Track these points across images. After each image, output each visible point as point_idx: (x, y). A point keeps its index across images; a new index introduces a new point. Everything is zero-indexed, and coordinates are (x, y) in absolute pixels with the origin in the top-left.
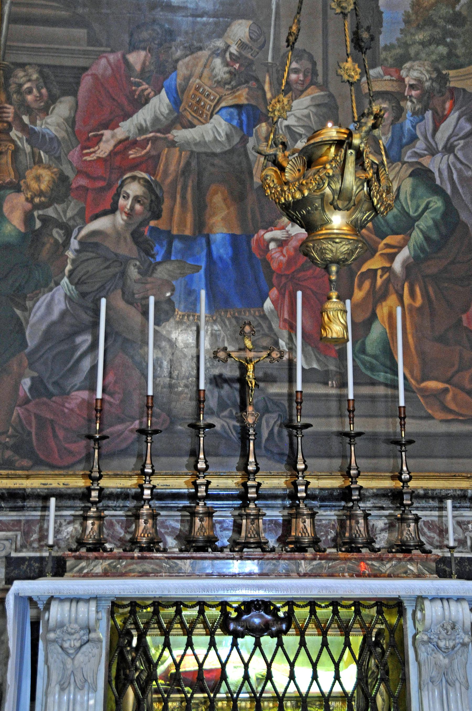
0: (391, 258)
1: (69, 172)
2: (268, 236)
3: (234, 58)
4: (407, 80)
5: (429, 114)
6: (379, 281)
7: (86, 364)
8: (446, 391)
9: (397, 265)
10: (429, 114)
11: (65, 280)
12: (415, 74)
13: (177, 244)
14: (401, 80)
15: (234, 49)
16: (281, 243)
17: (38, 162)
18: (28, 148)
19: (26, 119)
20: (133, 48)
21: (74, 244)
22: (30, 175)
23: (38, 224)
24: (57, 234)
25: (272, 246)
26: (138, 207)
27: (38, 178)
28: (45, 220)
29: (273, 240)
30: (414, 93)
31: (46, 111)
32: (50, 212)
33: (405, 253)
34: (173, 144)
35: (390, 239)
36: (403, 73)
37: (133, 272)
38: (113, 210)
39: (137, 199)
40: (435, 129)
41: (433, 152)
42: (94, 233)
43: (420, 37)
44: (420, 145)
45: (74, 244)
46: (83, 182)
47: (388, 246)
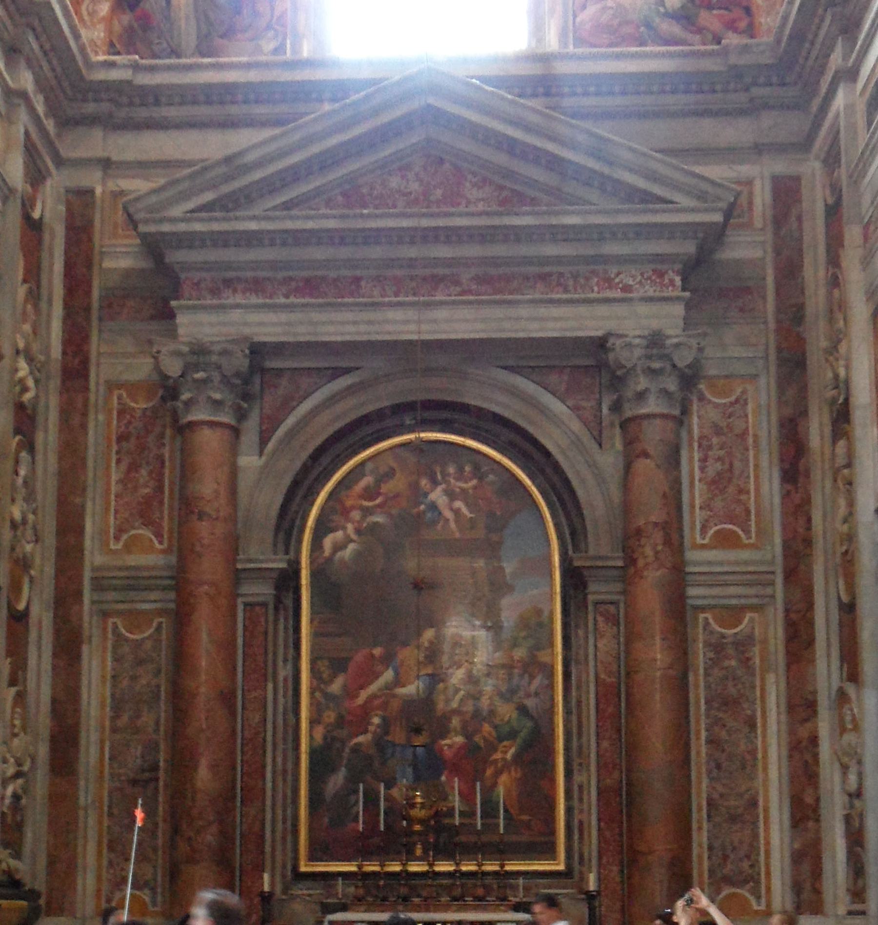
0: (506, 752)
1: (344, 713)
2: (444, 742)
3: (427, 649)
4: (515, 657)
5: (526, 676)
6: (499, 765)
7: (354, 810)
8: (530, 820)
9: (509, 756)
10: (526, 676)
11: (343, 769)
12: (520, 654)
13: (398, 749)
14: (512, 657)
15: (426, 644)
16: (450, 746)
17: (328, 708)
18: (323, 701)
19: (322, 686)
20: (375, 646)
21: (347, 750)
22: (326, 714)
23: (329, 740)
24: (338, 745)
25: (446, 748)
26: (378, 730)
27: (329, 717)
28: (333, 739)
29: (446, 745)
30: (519, 664)
31: (331, 681)
32: (335, 734)
33: (512, 751)
34: (394, 696)
35: (505, 743)
36: (514, 654)
37: (376, 764)
38: (365, 732)
39: (378, 726)
40: (530, 683)
41: (528, 695)
42: (355, 744)
43: (523, 634)
44: (521, 693)
45: (347, 750)
46: (351, 718)
47: (505, 747)
